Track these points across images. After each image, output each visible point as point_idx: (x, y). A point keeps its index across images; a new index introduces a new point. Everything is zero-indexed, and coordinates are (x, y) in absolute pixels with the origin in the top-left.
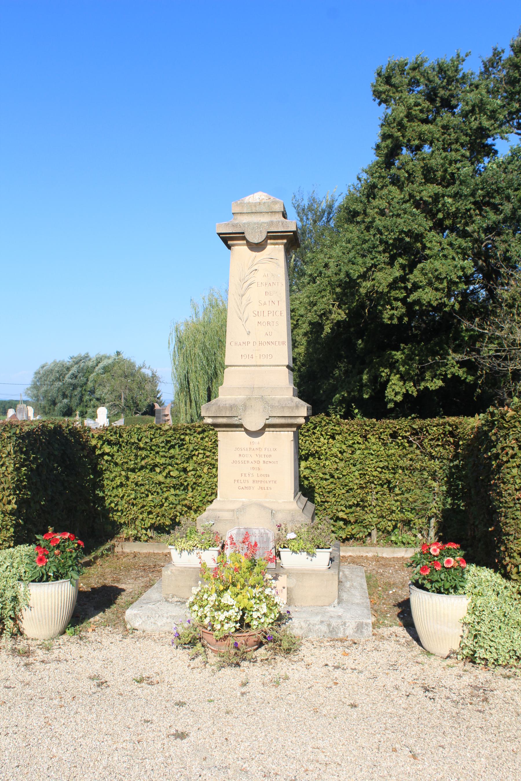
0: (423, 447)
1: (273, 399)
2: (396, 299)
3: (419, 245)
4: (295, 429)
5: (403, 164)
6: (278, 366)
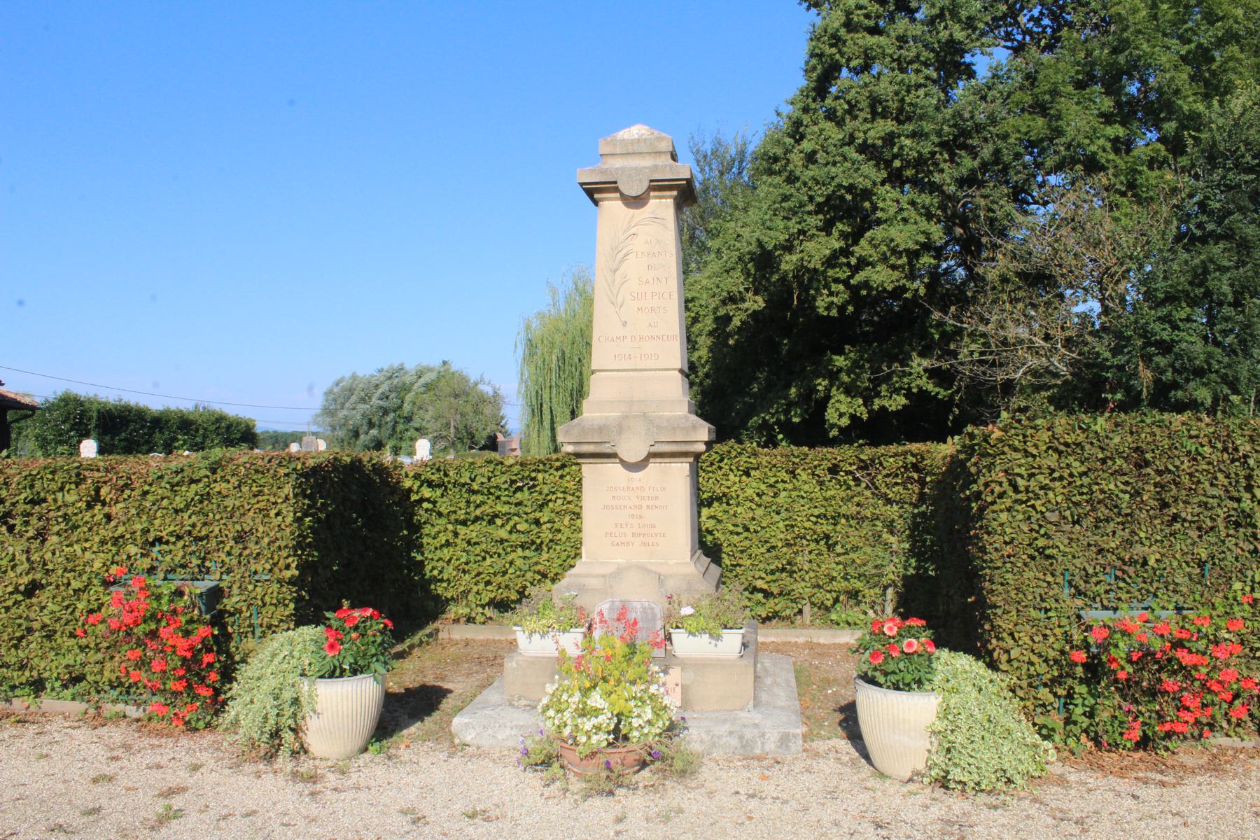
0: (877, 488)
1: (660, 417)
2: (837, 281)
3: (867, 204)
4: (691, 460)
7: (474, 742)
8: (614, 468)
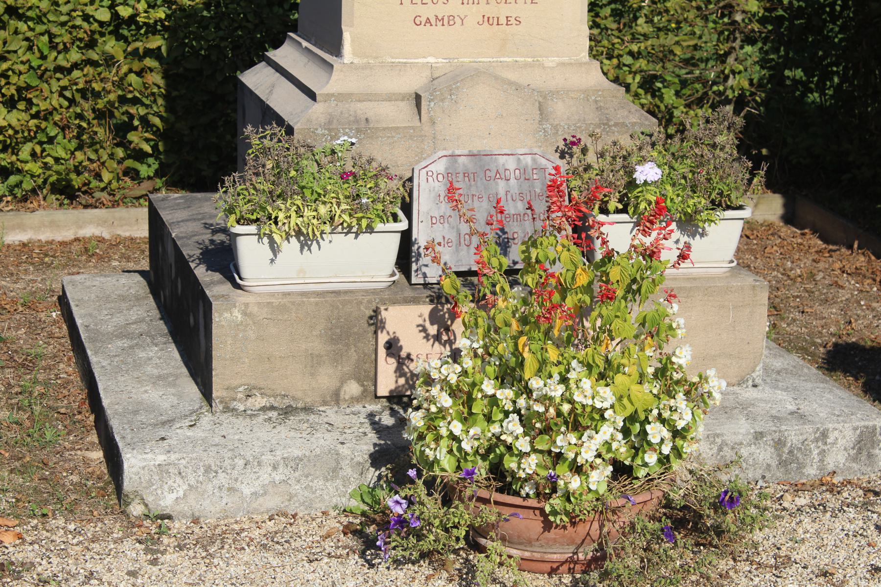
7: (183, 507)
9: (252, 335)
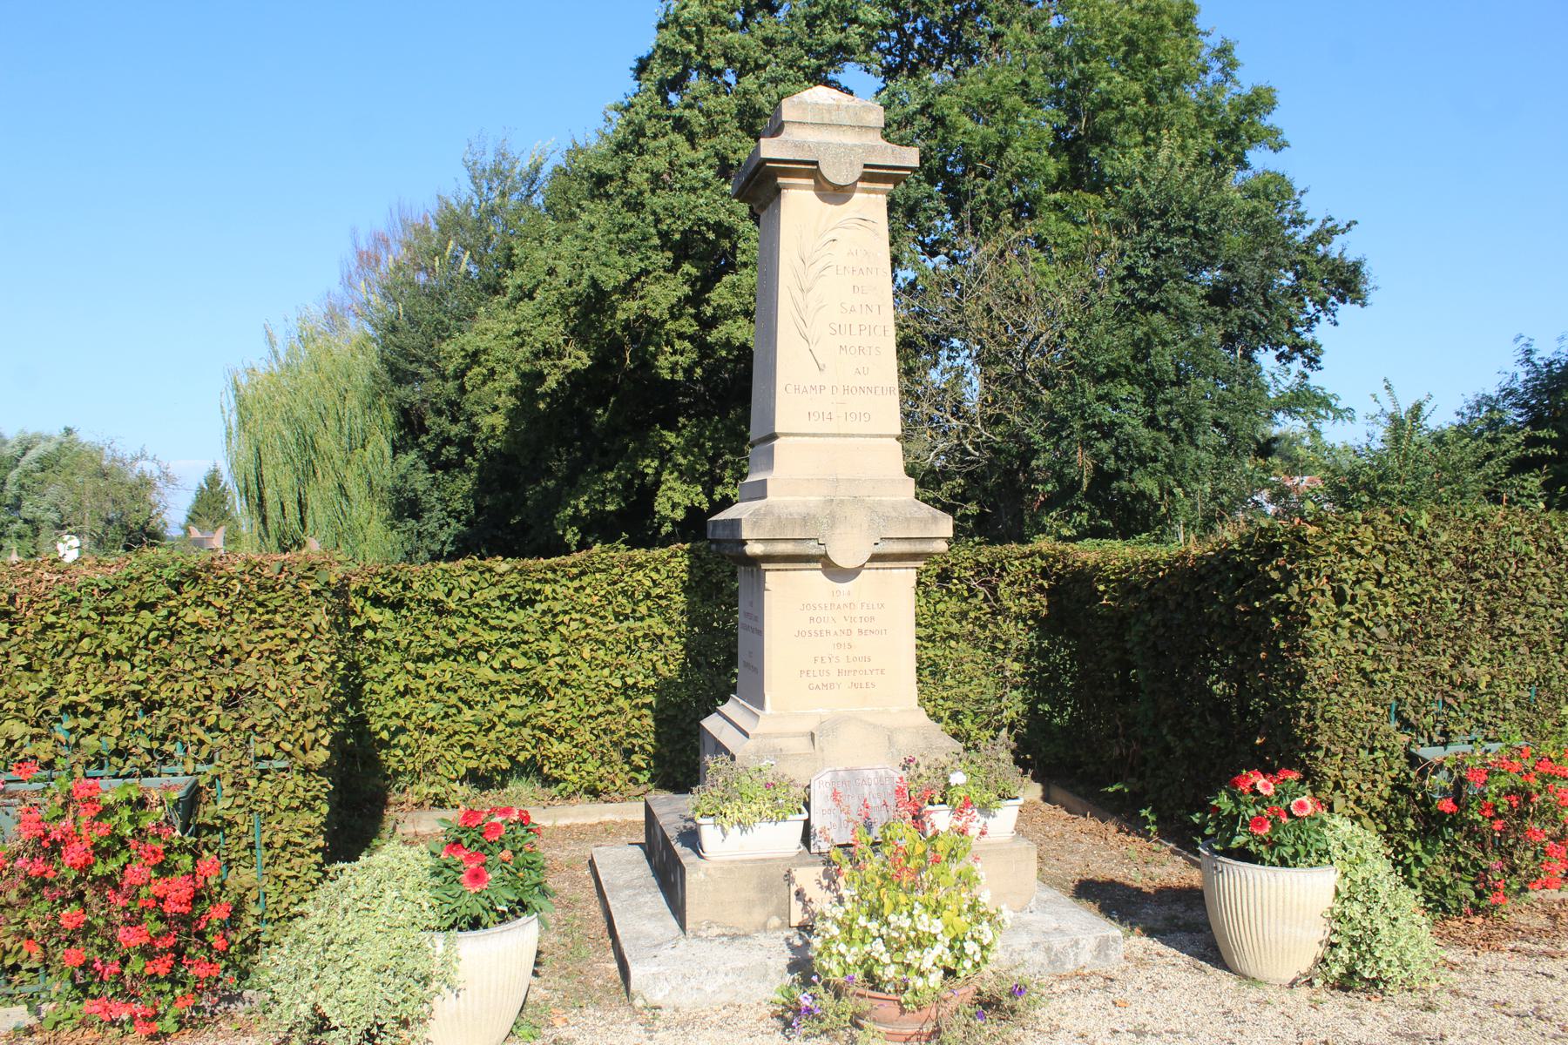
0: (997, 600)
1: (880, 503)
2: (681, 336)
3: (726, 244)
4: (921, 565)
5: (695, 98)
6: (881, 436)
8: (813, 577)
9: (710, 888)
